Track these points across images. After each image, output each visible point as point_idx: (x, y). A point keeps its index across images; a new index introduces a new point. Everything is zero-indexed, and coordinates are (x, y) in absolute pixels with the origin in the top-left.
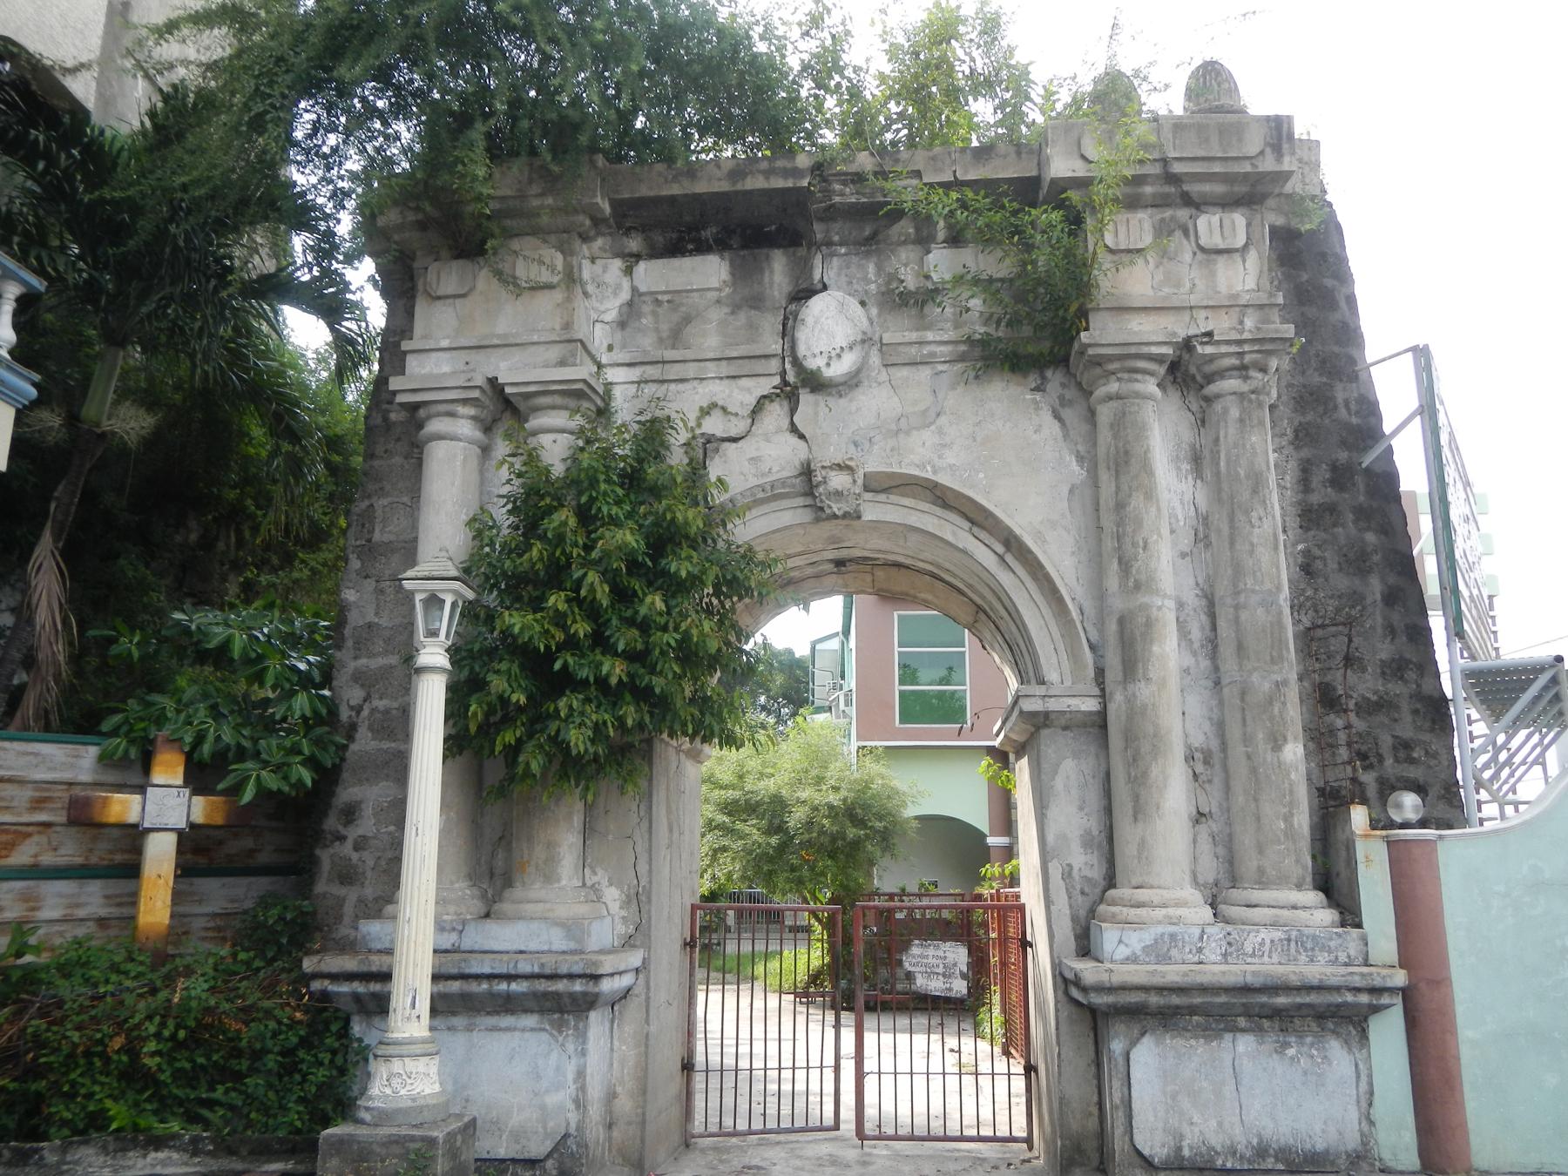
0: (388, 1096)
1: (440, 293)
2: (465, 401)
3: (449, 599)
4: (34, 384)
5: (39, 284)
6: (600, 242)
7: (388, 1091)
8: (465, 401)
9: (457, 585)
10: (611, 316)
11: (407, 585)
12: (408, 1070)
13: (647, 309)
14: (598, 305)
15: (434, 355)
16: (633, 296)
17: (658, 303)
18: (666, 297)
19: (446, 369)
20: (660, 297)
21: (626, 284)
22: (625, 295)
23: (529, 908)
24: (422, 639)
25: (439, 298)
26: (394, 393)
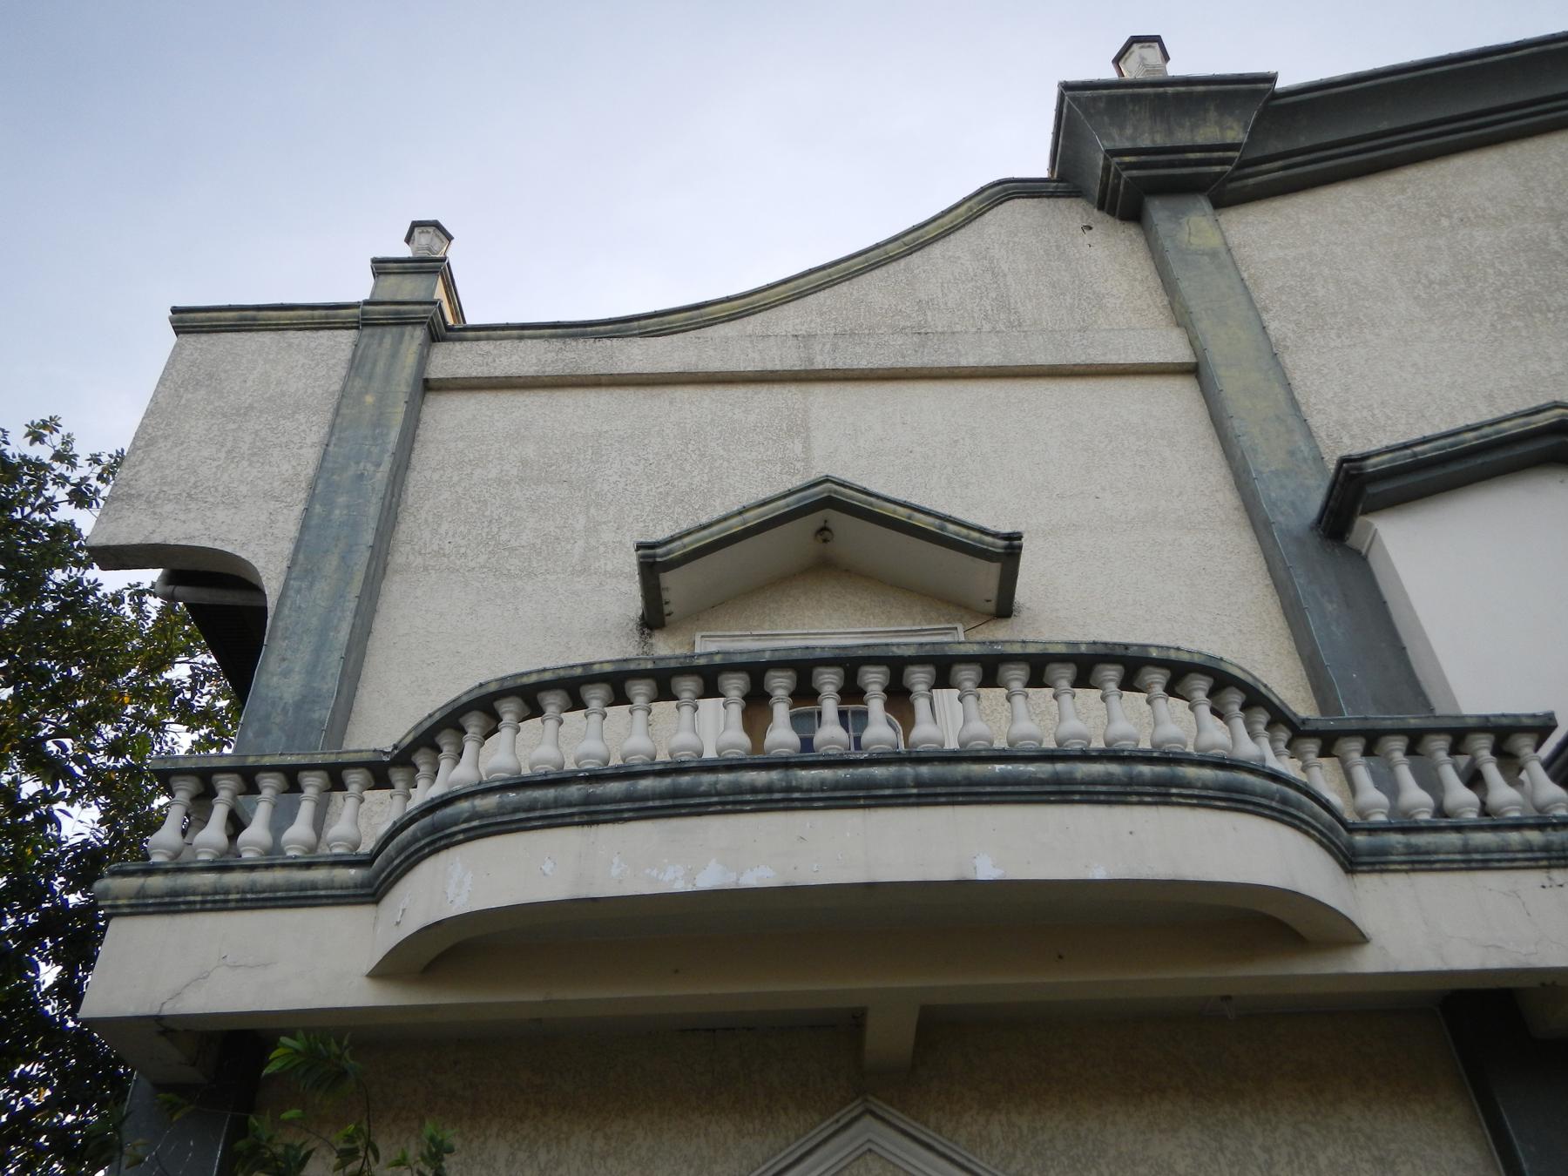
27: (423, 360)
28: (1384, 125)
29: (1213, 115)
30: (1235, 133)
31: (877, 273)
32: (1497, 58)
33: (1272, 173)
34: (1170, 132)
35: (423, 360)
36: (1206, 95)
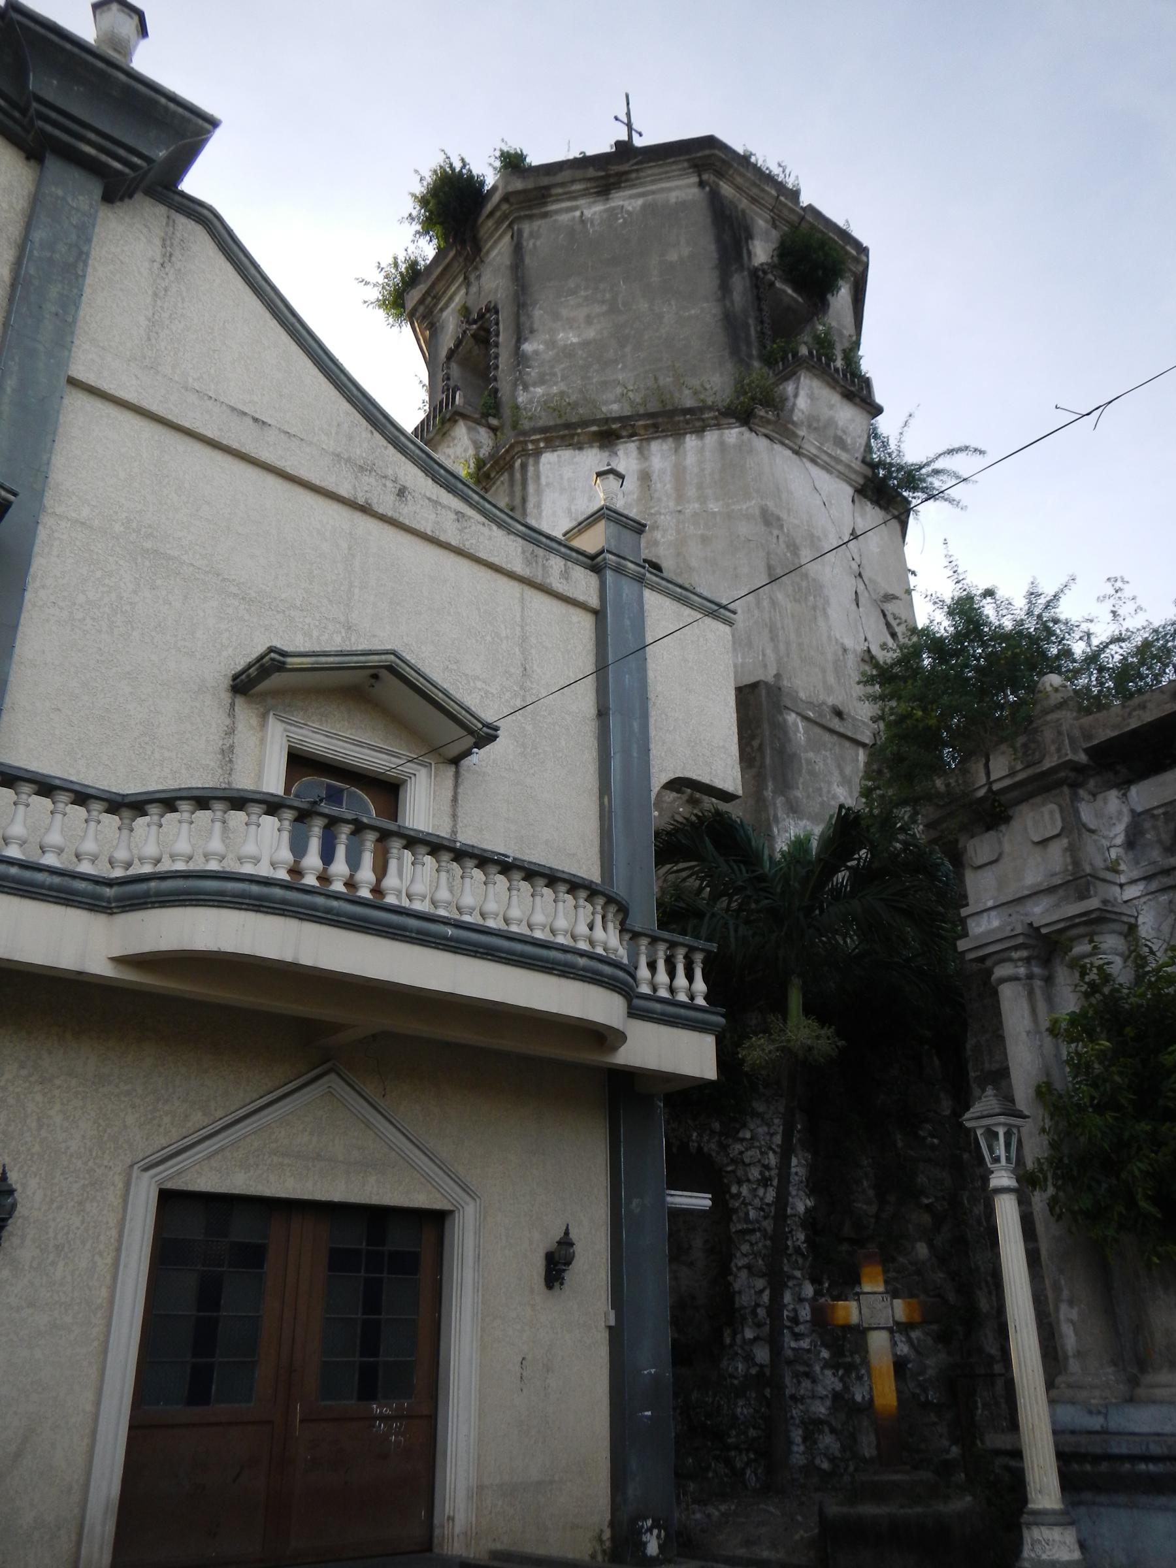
0: (1033, 1559)
1: (980, 862)
2: (1016, 948)
3: (1001, 1132)
4: (723, 1016)
5: (714, 947)
6: (1091, 783)
7: (1033, 1555)
8: (1016, 948)
9: (1002, 1119)
10: (1119, 840)
11: (968, 1124)
12: (1045, 1537)
13: (1147, 825)
14: (1108, 833)
15: (985, 914)
16: (1133, 817)
17: (1154, 816)
18: (1161, 811)
19: (996, 923)
20: (1155, 812)
21: (1125, 810)
22: (1126, 819)
23: (1159, 1393)
24: (989, 1166)
25: (980, 867)
26: (964, 952)
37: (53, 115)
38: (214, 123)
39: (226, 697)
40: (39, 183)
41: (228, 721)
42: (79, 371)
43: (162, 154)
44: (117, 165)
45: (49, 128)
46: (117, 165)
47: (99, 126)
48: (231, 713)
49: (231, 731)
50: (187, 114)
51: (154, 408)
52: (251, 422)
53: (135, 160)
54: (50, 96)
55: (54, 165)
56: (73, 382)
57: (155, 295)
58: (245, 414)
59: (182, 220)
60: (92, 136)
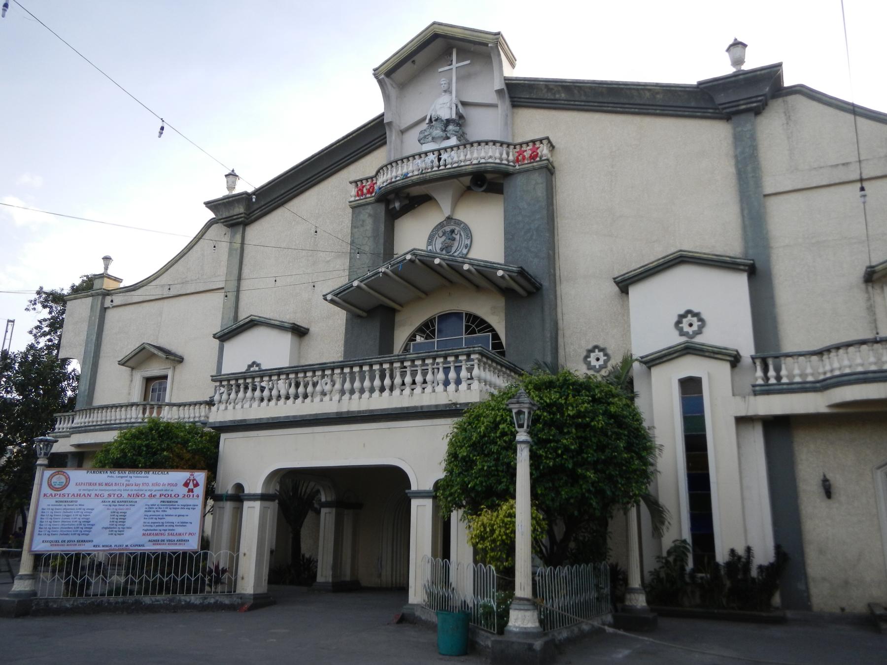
27: (102, 303)
28: (283, 192)
29: (236, 205)
30: (242, 210)
31: (183, 259)
32: (307, 163)
33: (257, 213)
34: (229, 212)
35: (102, 303)
36: (233, 201)
37: (727, 105)
38: (780, 65)
39: (863, 286)
40: (734, 129)
41: (866, 296)
42: (768, 190)
43: (767, 89)
44: (755, 105)
45: (728, 110)
46: (755, 105)
47: (743, 97)
48: (867, 292)
49: (869, 299)
50: (769, 70)
51: (799, 187)
52: (841, 167)
53: (760, 98)
54: (724, 101)
55: (735, 119)
56: (765, 196)
57: (788, 138)
58: (837, 165)
59: (791, 99)
60: (742, 102)
